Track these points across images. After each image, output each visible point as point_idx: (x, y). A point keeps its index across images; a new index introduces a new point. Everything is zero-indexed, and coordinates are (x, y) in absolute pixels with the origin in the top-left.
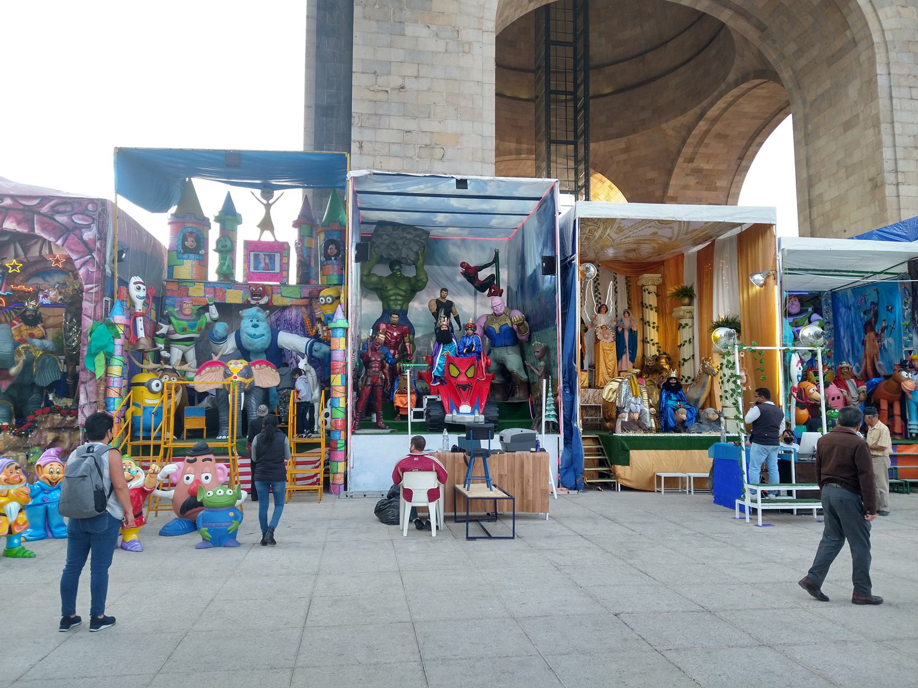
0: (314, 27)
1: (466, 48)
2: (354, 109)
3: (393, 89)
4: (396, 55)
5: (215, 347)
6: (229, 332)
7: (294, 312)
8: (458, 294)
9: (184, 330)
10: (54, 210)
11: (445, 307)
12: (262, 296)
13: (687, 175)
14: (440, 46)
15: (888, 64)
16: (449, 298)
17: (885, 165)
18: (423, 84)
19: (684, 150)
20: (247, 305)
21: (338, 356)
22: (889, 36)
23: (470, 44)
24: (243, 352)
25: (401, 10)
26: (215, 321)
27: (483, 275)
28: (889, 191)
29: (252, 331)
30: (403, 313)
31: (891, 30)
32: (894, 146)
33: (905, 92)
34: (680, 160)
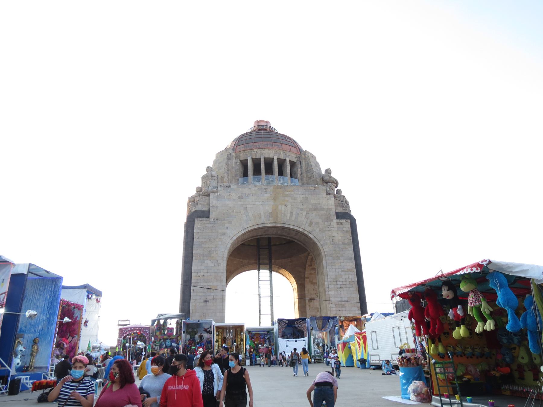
0: (184, 262)
1: (219, 265)
2: (192, 281)
3: (201, 276)
4: (202, 268)
5: (163, 346)
6: (164, 343)
7: (175, 339)
8: (204, 333)
9: (158, 344)
10: (143, 329)
11: (201, 337)
12: (169, 337)
13: (311, 270)
14: (213, 265)
15: (326, 260)
16: (202, 334)
17: (326, 286)
18: (209, 274)
19: (307, 263)
20: (167, 339)
21: (180, 348)
22: (326, 253)
23: (220, 264)
24: (166, 347)
25: (204, 257)
26: (162, 342)
27: (208, 330)
28: (327, 293)
29: (168, 343)
30: (194, 338)
31: (326, 252)
32: (328, 281)
33: (330, 267)
34: (307, 266)
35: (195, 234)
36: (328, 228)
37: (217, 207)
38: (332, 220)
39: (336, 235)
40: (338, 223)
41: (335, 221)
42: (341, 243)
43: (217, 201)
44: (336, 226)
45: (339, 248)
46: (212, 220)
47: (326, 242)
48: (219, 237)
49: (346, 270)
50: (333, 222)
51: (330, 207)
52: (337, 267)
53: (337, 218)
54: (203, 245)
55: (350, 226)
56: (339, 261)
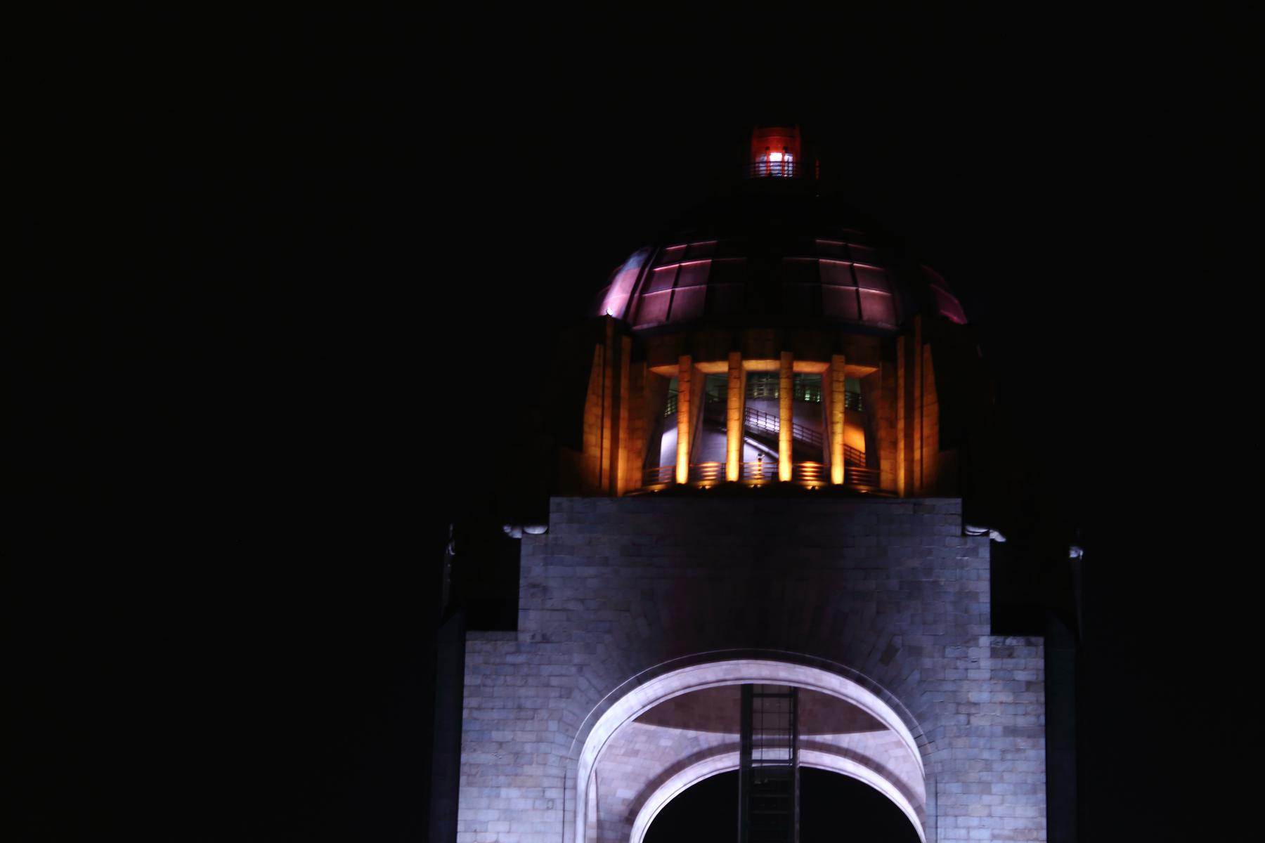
14: (529, 804)
23: (553, 800)
33: (950, 820)
35: (466, 693)
36: (956, 668)
37: (545, 590)
38: (974, 639)
39: (985, 697)
40: (994, 653)
41: (985, 641)
42: (999, 729)
43: (546, 564)
44: (986, 663)
45: (991, 749)
46: (525, 637)
47: (945, 726)
48: (552, 704)
49: (1011, 834)
50: (977, 646)
51: (972, 586)
52: (974, 822)
53: (995, 631)
54: (496, 735)
55: (1041, 663)
56: (986, 799)
